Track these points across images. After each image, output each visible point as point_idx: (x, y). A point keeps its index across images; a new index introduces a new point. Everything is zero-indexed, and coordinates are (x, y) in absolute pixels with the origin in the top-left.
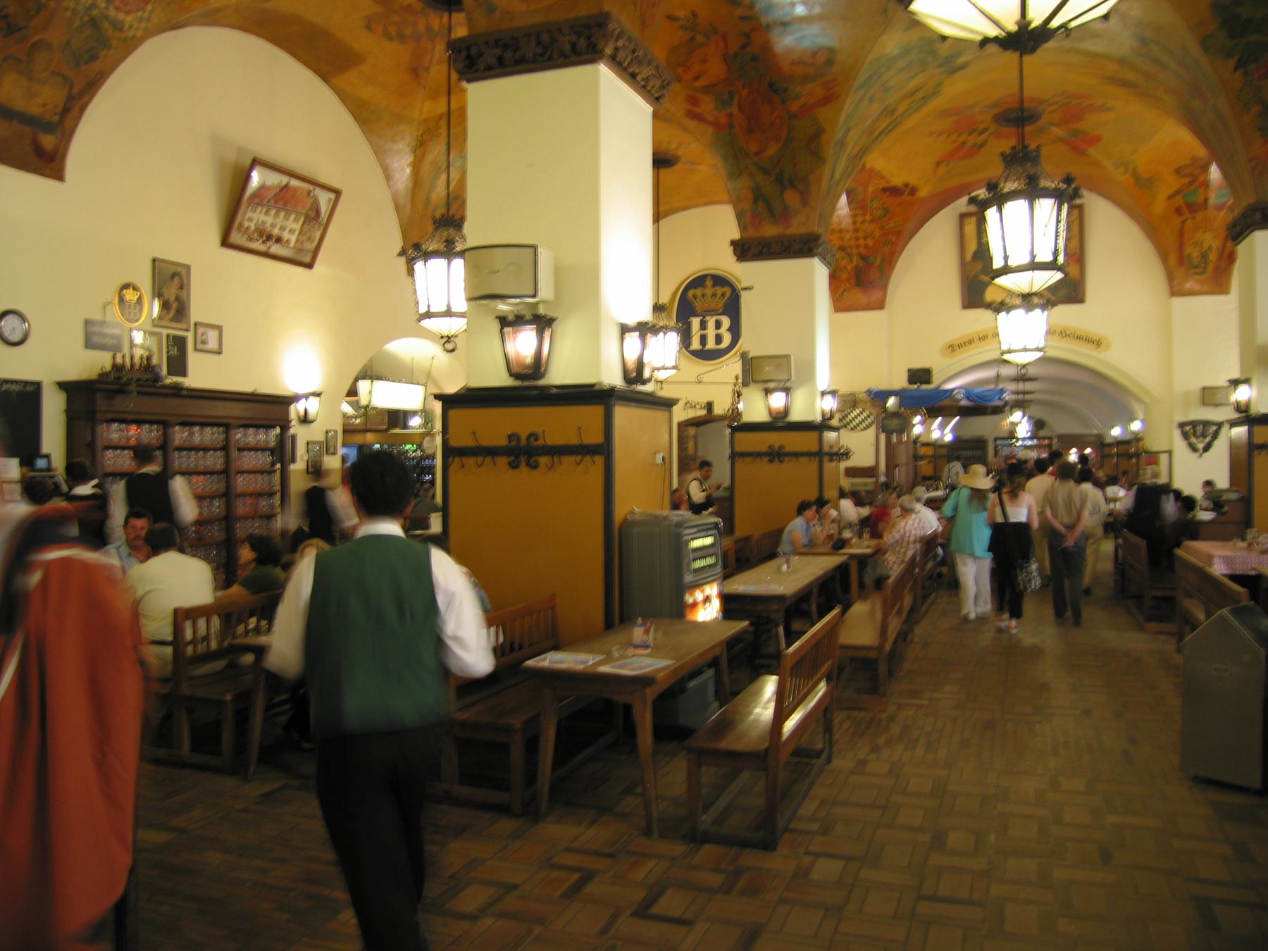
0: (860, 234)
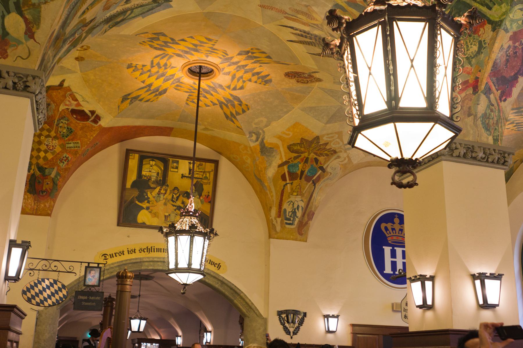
0: (43, 147)
